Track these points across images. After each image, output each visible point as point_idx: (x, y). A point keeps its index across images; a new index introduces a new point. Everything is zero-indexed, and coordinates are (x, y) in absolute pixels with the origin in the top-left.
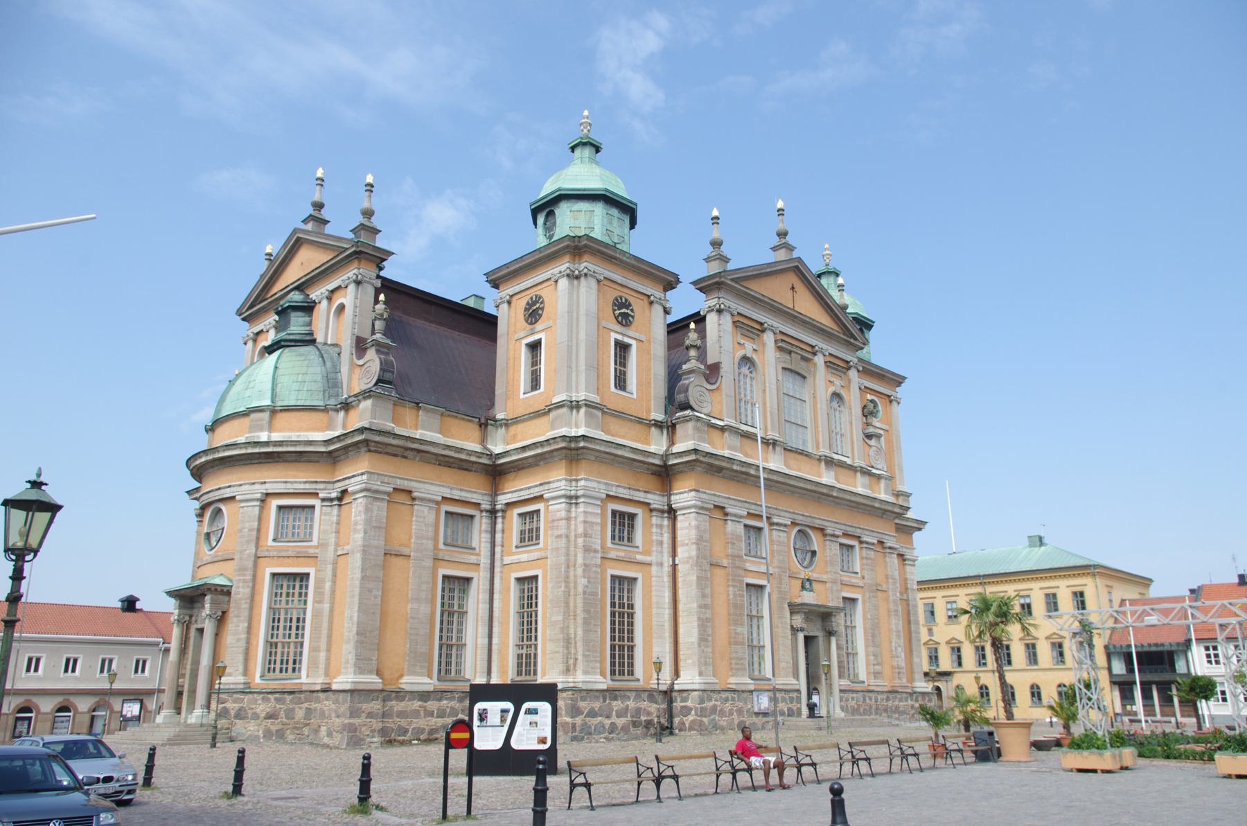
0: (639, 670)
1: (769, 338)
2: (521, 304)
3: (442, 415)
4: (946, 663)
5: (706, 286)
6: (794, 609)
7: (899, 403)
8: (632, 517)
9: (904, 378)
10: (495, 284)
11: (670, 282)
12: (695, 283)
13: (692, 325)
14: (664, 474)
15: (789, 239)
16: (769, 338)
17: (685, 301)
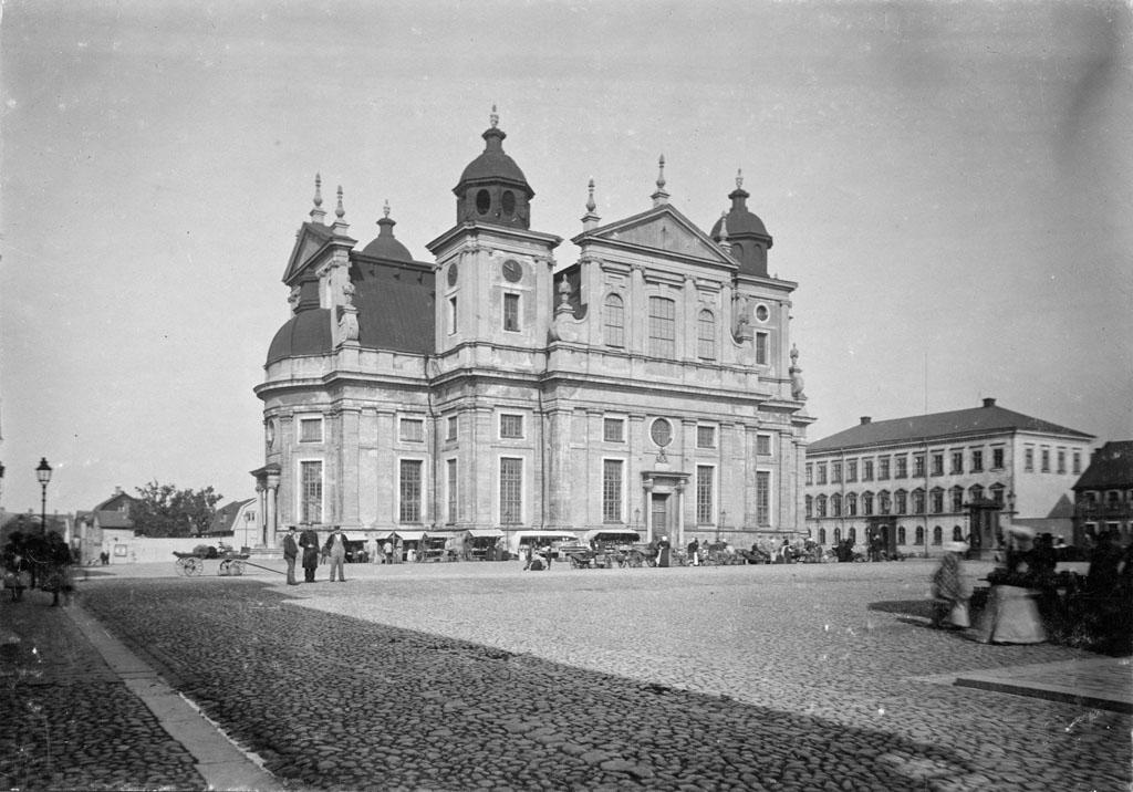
0: (624, 517)
1: (637, 274)
2: (446, 268)
3: (395, 355)
4: (894, 510)
5: (581, 241)
6: (645, 475)
7: (790, 306)
8: (520, 417)
9: (796, 284)
10: (435, 252)
11: (553, 244)
12: (572, 240)
13: (565, 276)
14: (546, 382)
15: (666, 189)
16: (637, 274)
17: (566, 256)
